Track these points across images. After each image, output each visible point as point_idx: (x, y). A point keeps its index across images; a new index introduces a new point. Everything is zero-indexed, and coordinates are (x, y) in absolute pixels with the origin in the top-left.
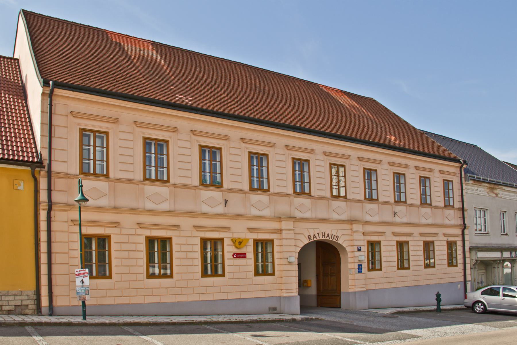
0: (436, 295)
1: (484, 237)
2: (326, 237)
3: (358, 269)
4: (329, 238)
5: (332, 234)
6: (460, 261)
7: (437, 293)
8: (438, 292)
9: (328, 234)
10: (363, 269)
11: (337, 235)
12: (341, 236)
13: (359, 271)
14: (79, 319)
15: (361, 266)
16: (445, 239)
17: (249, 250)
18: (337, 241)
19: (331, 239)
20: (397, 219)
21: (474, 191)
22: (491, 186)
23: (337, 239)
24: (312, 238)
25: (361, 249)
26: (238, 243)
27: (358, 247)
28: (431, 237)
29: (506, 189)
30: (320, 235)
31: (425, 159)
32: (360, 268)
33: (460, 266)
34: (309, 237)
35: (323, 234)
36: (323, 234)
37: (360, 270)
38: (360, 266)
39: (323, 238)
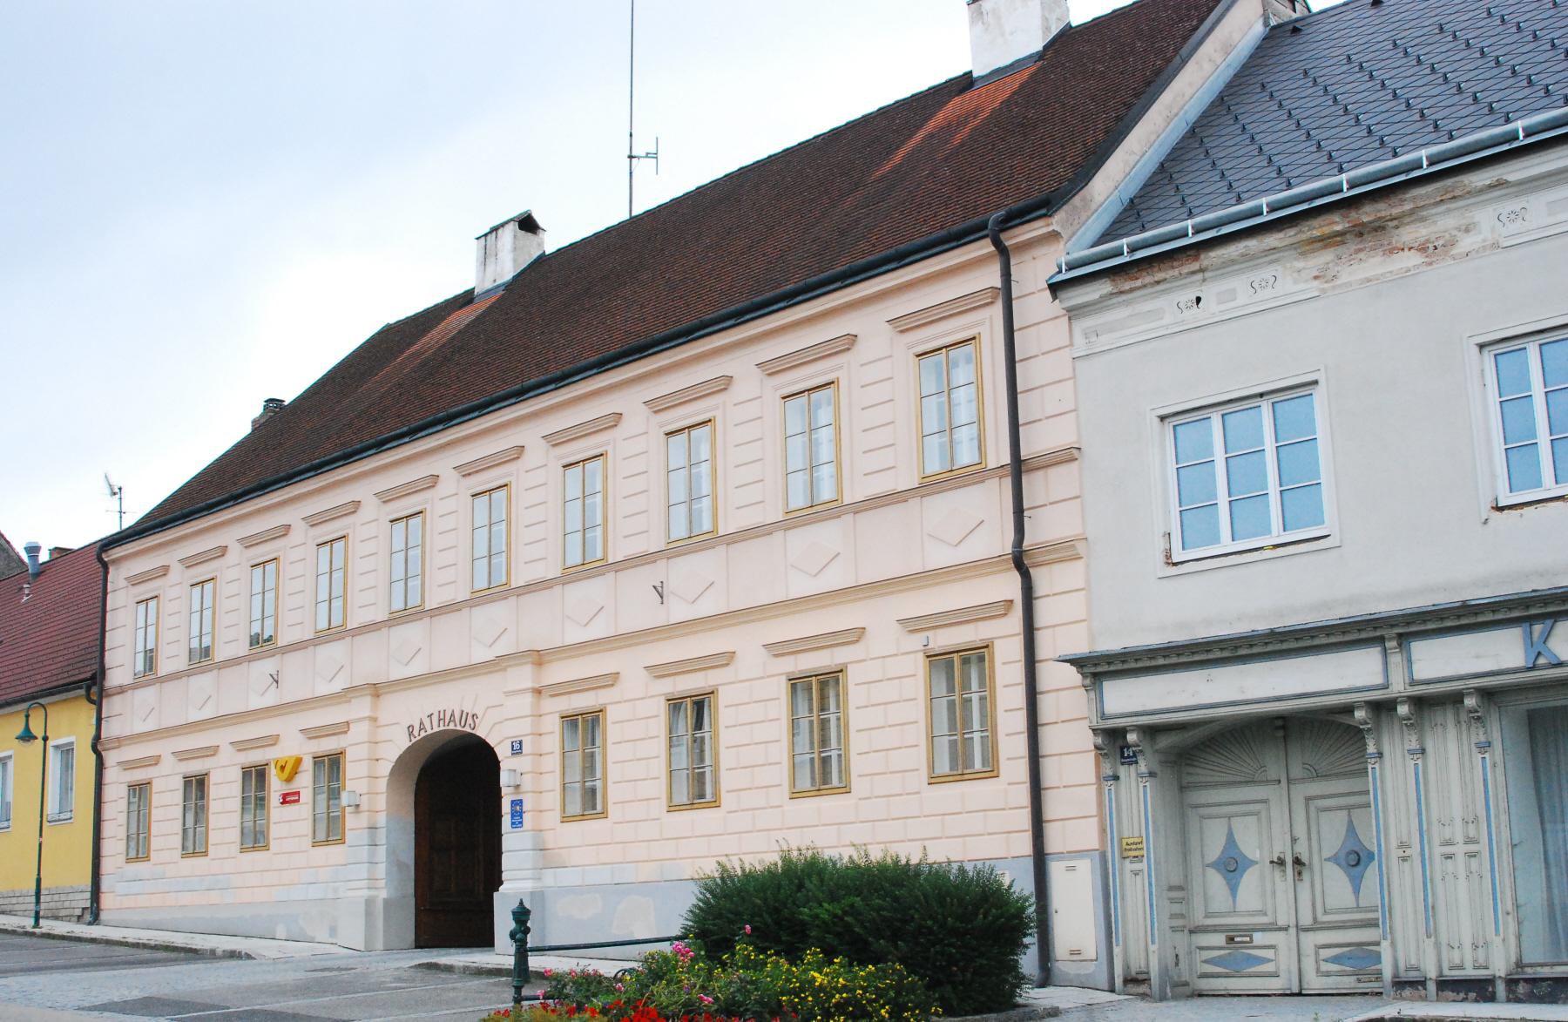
0: (514, 913)
1: (1260, 566)
2: (446, 724)
3: (512, 818)
4: (456, 726)
5: (463, 711)
6: (1013, 747)
7: (515, 905)
8: (521, 900)
9: (452, 715)
10: (525, 816)
11: (474, 713)
12: (486, 711)
13: (513, 823)
14: (28, 923)
15: (521, 806)
16: (917, 641)
17: (304, 782)
18: (473, 732)
19: (459, 728)
20: (679, 611)
21: (1167, 319)
22: (1304, 237)
23: (472, 726)
24: (416, 732)
25: (521, 749)
26: (291, 770)
27: (512, 743)
28: (700, 675)
29: (1512, 178)
30: (435, 718)
31: (856, 292)
32: (517, 812)
33: (1014, 766)
34: (411, 730)
35: (442, 717)
36: (442, 717)
37: (517, 819)
38: (517, 804)
39: (442, 728)
